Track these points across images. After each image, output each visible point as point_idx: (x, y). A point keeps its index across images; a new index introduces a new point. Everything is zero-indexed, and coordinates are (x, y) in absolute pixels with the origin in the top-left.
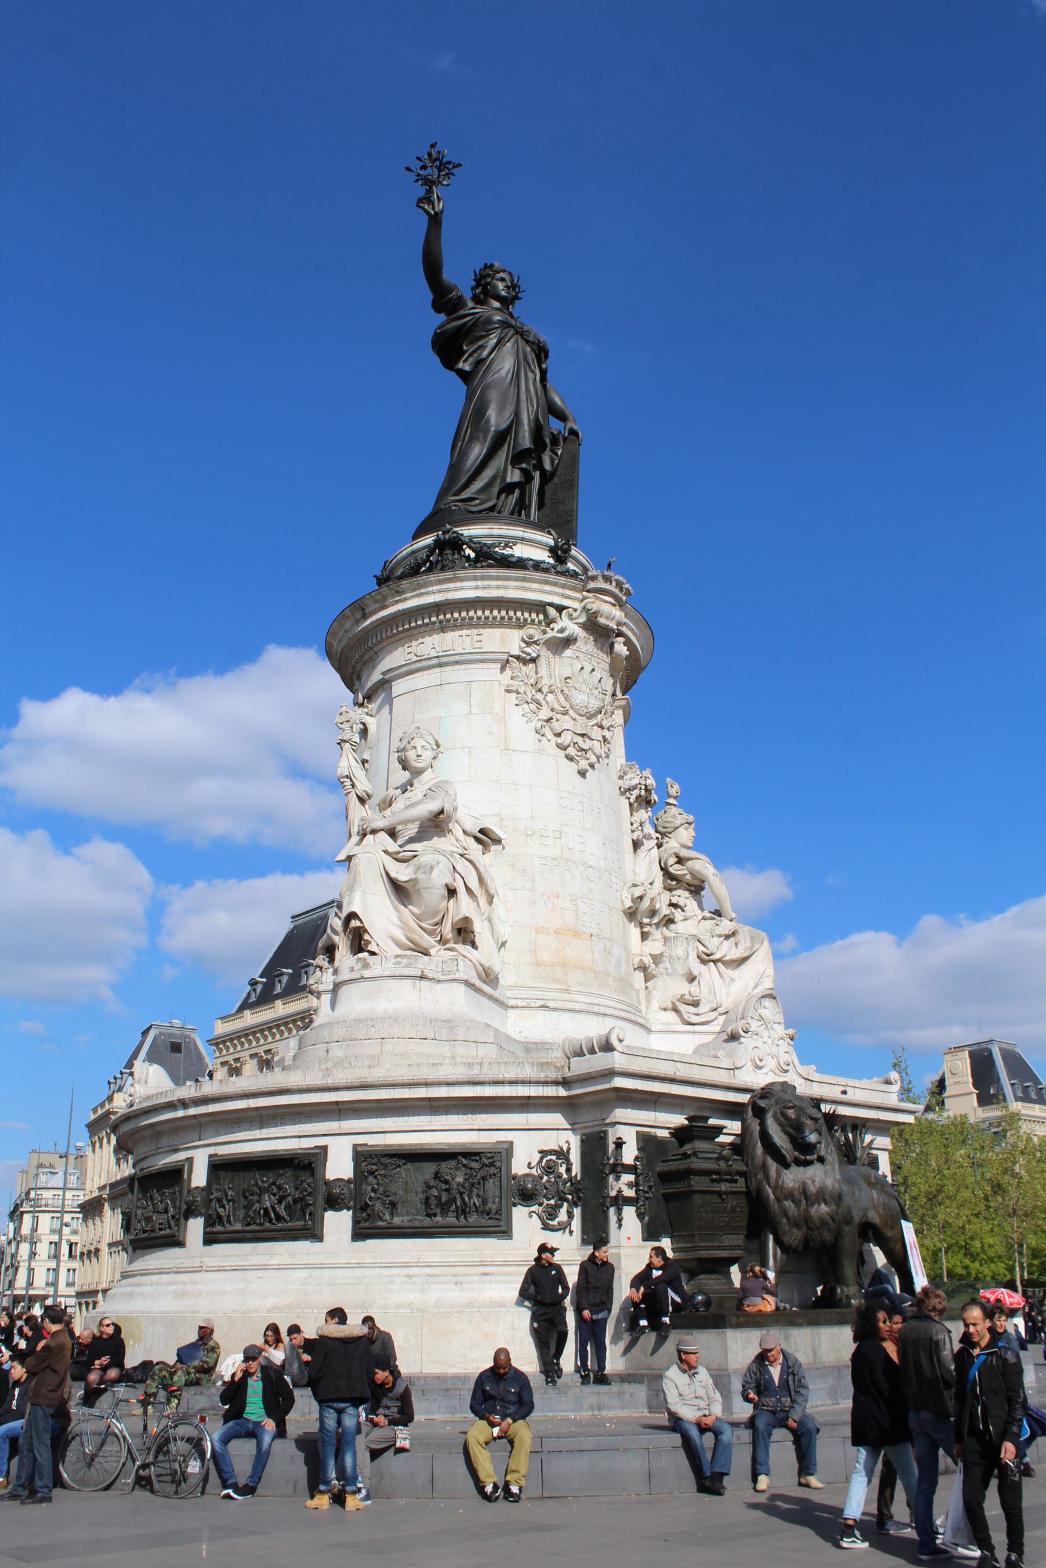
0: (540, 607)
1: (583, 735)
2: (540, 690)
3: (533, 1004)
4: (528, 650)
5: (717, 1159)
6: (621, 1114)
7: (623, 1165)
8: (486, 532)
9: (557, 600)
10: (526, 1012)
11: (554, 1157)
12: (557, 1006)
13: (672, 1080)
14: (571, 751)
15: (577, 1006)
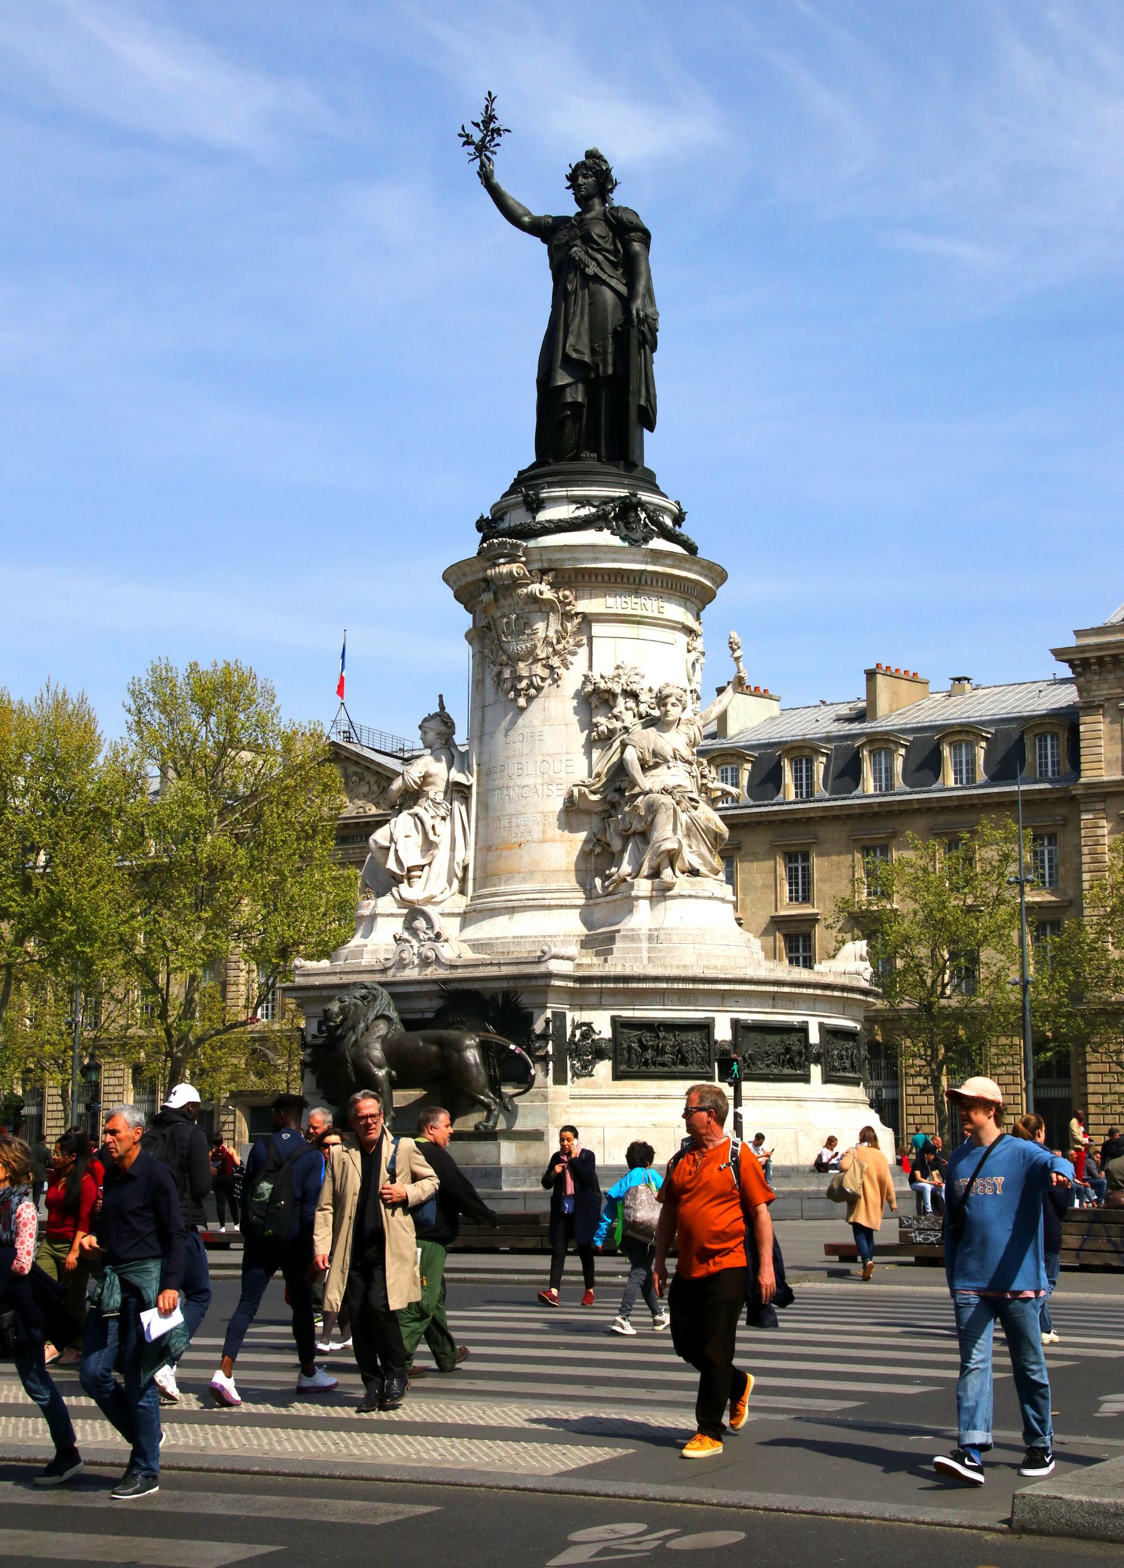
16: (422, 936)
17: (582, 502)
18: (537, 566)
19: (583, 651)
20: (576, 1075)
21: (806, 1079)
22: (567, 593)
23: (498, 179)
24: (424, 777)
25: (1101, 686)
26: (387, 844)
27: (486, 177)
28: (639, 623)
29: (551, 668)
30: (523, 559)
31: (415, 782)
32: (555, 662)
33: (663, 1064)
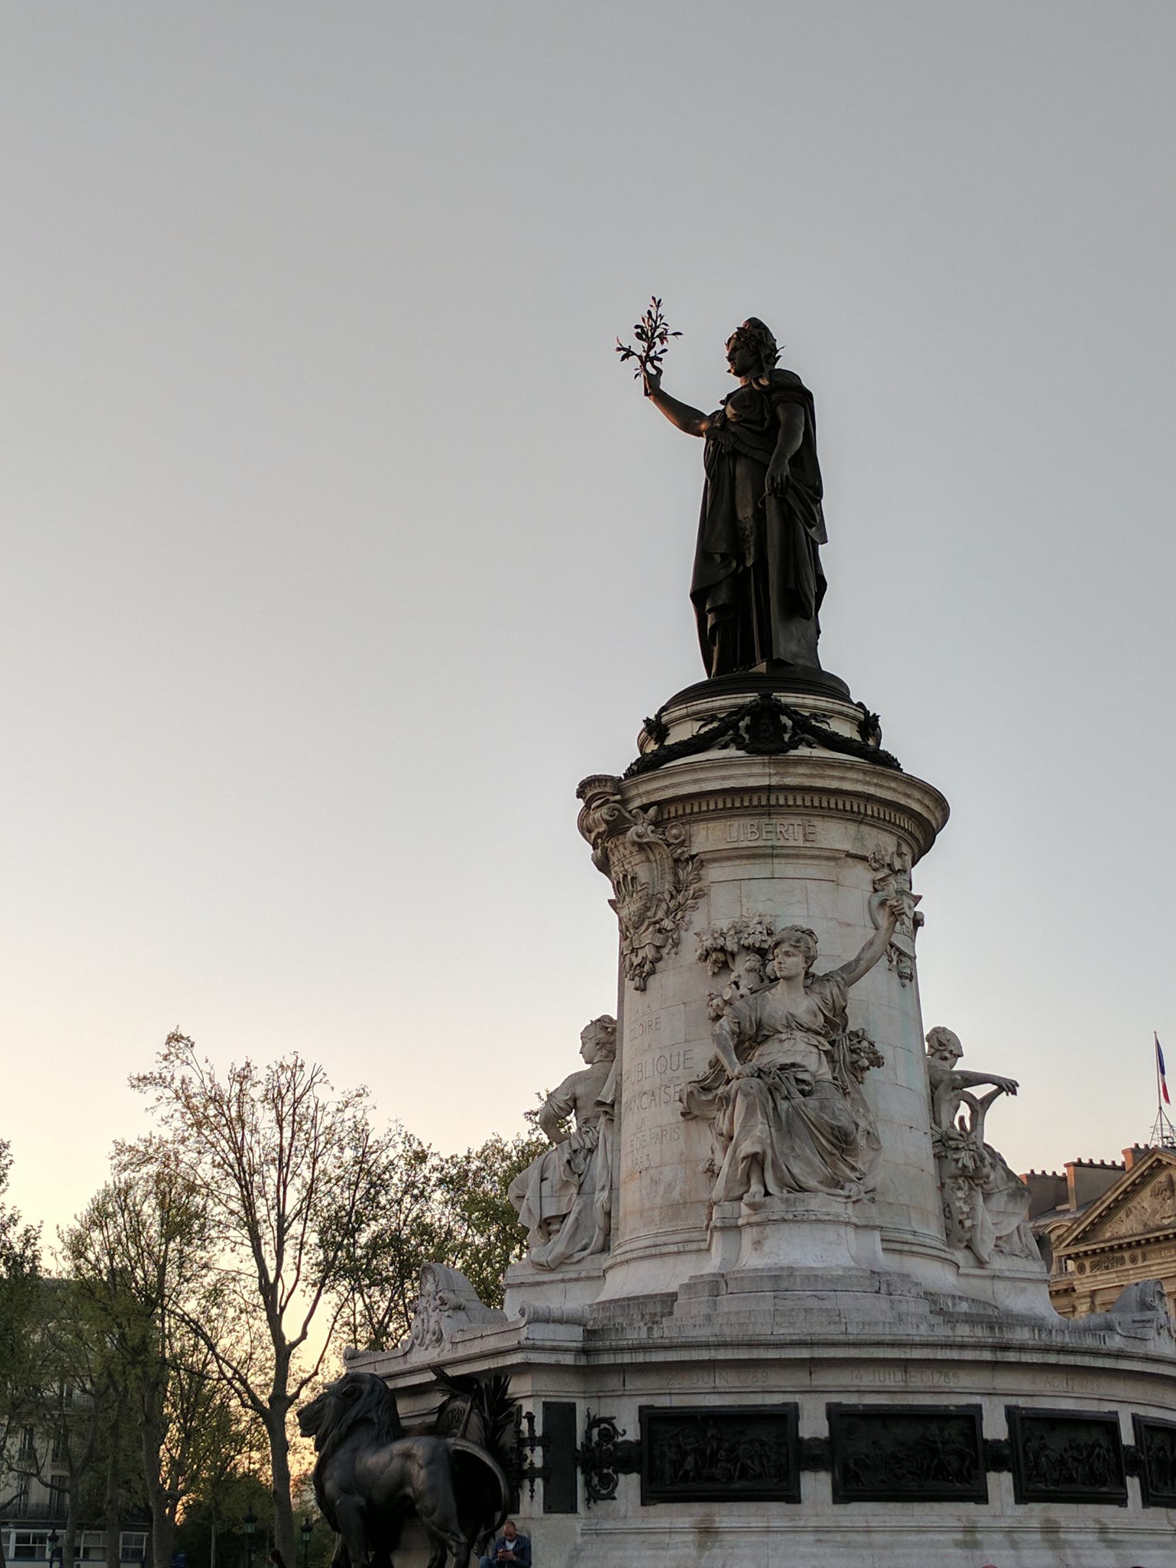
18: (637, 803)
20: (594, 1497)
21: (981, 1498)
22: (674, 831)
23: (666, 385)
27: (653, 388)
28: (772, 856)
30: (618, 797)
32: (667, 924)
33: (712, 1478)
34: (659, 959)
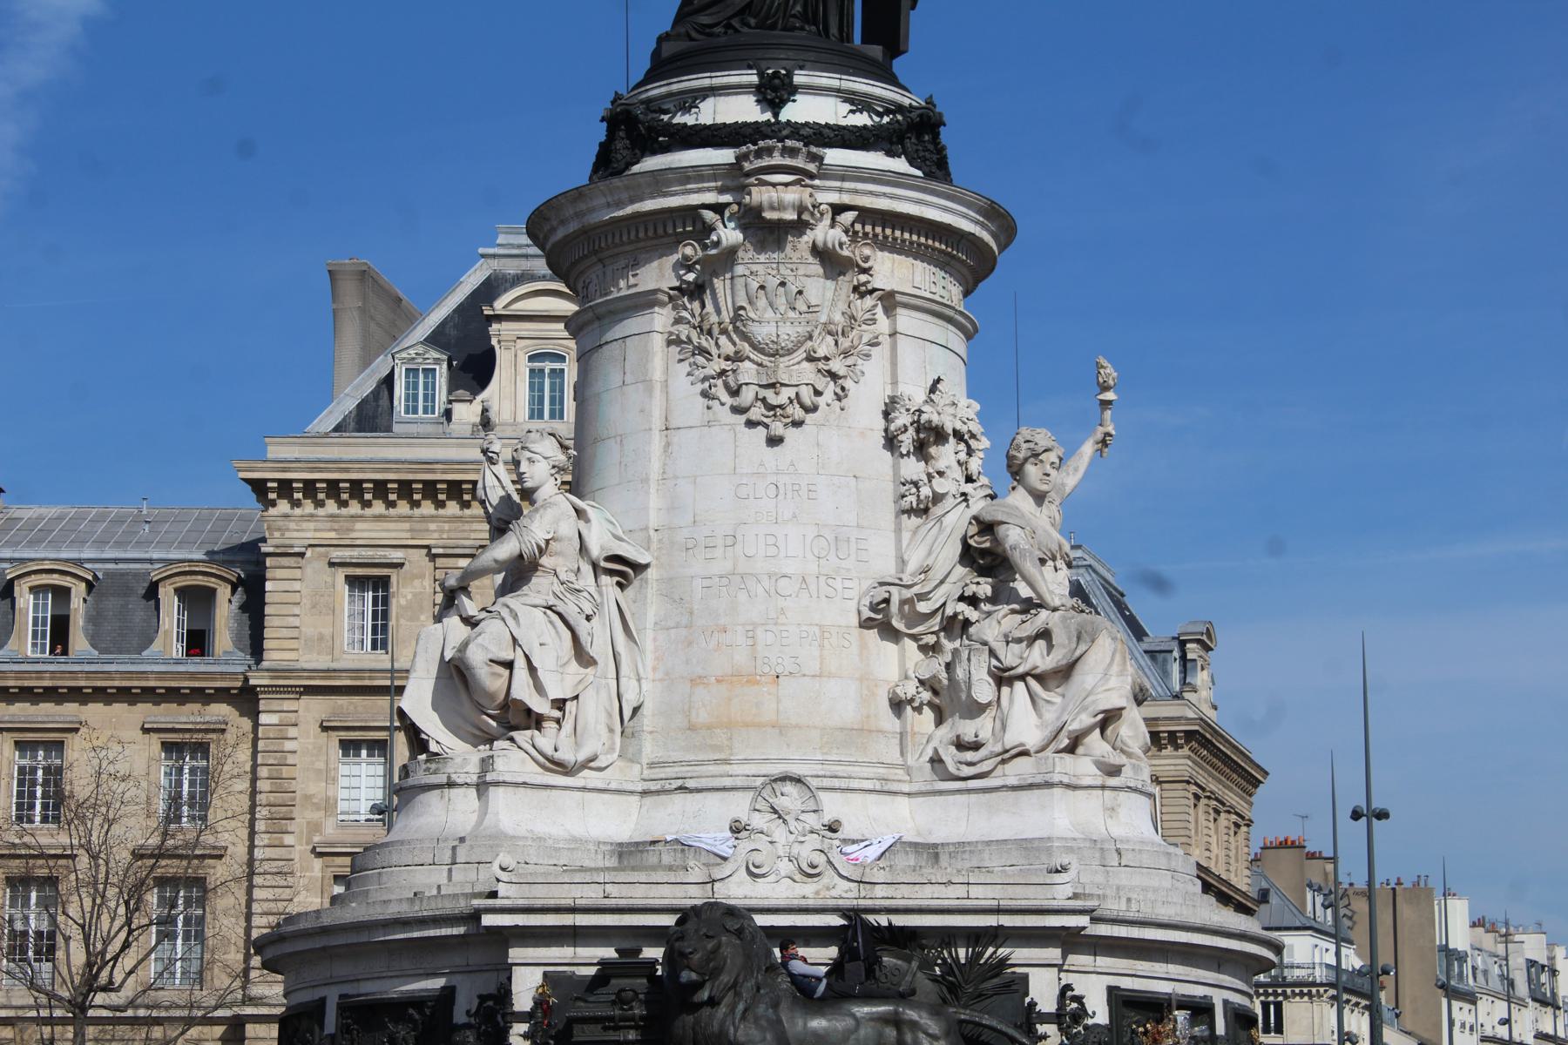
0: (692, 212)
1: (773, 386)
2: (710, 333)
3: (667, 787)
4: (691, 277)
5: (613, 1003)
6: (515, 954)
7: (514, 1013)
8: (663, 90)
9: (711, 198)
10: (663, 797)
11: (491, 1003)
12: (699, 786)
13: (573, 910)
14: (757, 413)
15: (728, 782)
16: (793, 824)
17: (859, 102)
18: (834, 198)
19: (880, 355)
22: (867, 251)
24: (547, 541)
25: (305, 525)
26: (507, 655)
29: (834, 376)
31: (539, 547)
32: (837, 366)
34: (814, 409)
